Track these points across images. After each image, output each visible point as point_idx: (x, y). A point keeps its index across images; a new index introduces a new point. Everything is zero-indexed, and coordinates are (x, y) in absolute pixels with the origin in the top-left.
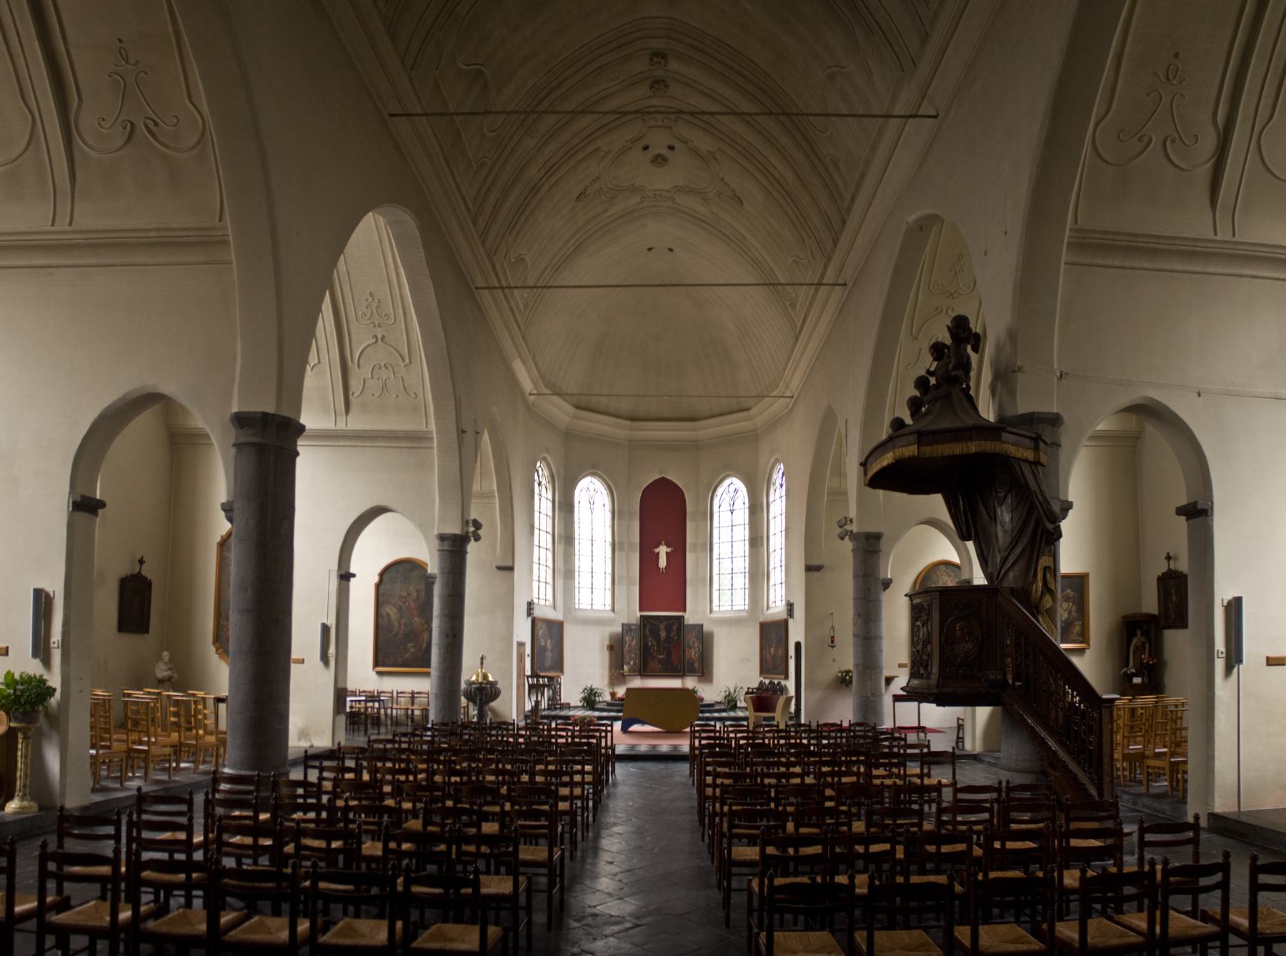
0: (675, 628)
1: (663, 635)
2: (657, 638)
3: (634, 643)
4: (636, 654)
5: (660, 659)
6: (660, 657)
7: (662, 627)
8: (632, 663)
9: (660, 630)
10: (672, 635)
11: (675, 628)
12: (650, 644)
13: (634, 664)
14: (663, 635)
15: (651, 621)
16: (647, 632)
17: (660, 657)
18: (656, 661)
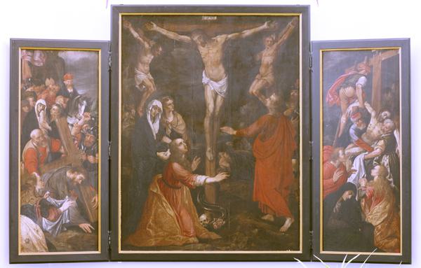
0: (267, 57)
1: (215, 86)
2: (192, 110)
3: (77, 121)
4: (89, 168)
5: (198, 191)
6: (200, 179)
7: (211, 53)
8: (67, 205)
9: (202, 66)
10: (255, 87)
11: (267, 57)
12: (155, 127)
13: (82, 210)
14: (215, 86)
15: (155, 27)
16: (143, 76)
17: (200, 179)
18: (184, 195)
